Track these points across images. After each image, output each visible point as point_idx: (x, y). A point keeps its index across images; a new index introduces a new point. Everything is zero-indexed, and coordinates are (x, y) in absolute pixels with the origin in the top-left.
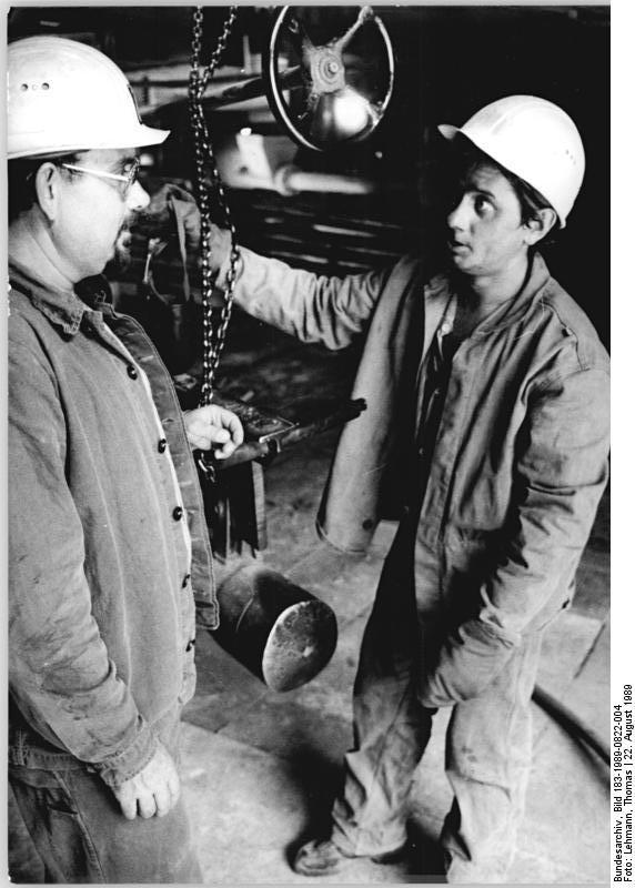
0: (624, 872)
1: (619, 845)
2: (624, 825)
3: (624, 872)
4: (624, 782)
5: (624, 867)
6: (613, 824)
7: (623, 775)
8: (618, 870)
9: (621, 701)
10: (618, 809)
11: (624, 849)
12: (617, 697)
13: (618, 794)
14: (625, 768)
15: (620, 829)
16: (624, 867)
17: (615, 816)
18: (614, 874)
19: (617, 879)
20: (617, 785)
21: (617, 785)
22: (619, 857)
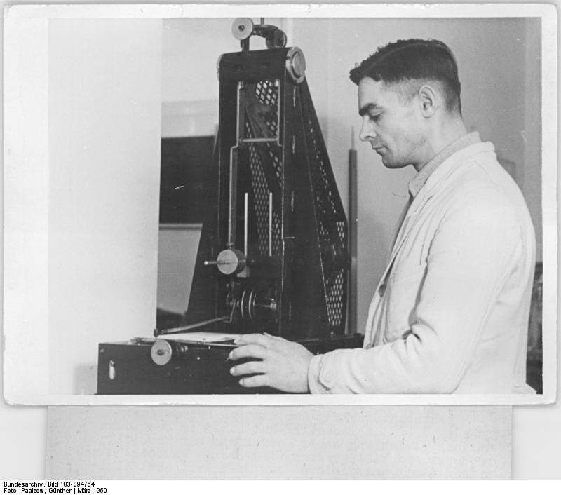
0: (10, 488)
1: (27, 485)
2: (40, 488)
3: (10, 488)
4: (66, 488)
5: (13, 488)
6: (41, 482)
7: (69, 488)
8: (11, 484)
9: (96, 487)
10: (49, 484)
11: (26, 488)
12: (99, 484)
13: (59, 484)
14: (72, 488)
15: (38, 485)
16: (13, 488)
17: (45, 482)
18: (9, 482)
19: (6, 484)
20: (65, 484)
21: (65, 485)
22: (20, 485)
